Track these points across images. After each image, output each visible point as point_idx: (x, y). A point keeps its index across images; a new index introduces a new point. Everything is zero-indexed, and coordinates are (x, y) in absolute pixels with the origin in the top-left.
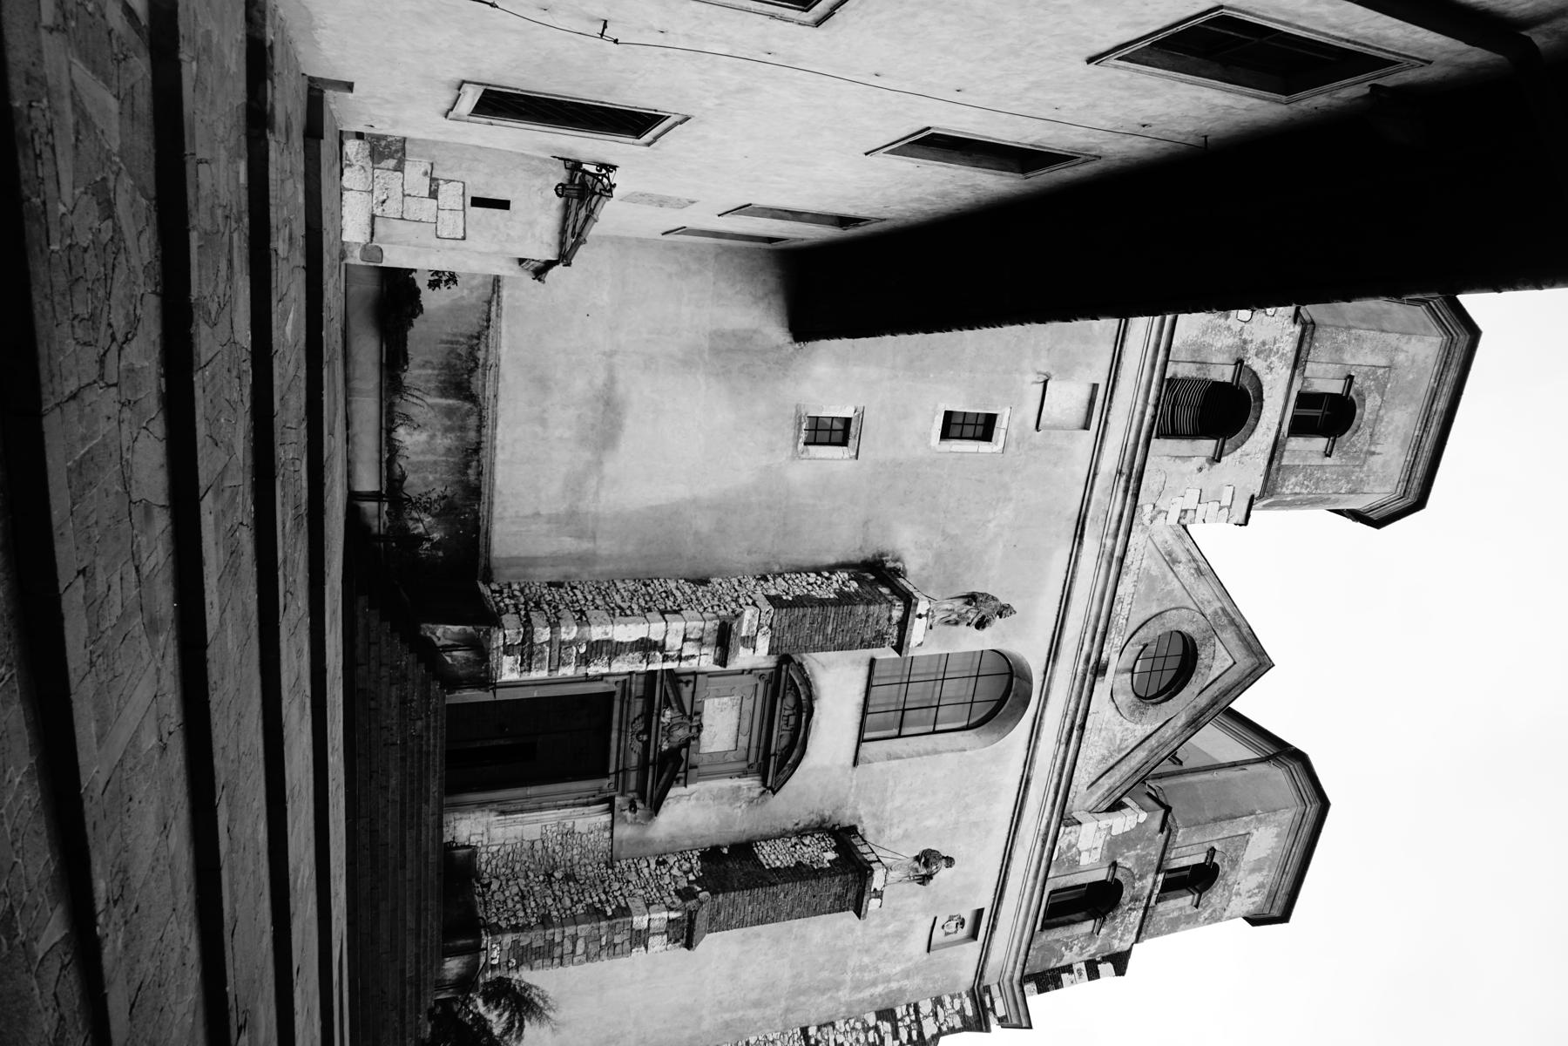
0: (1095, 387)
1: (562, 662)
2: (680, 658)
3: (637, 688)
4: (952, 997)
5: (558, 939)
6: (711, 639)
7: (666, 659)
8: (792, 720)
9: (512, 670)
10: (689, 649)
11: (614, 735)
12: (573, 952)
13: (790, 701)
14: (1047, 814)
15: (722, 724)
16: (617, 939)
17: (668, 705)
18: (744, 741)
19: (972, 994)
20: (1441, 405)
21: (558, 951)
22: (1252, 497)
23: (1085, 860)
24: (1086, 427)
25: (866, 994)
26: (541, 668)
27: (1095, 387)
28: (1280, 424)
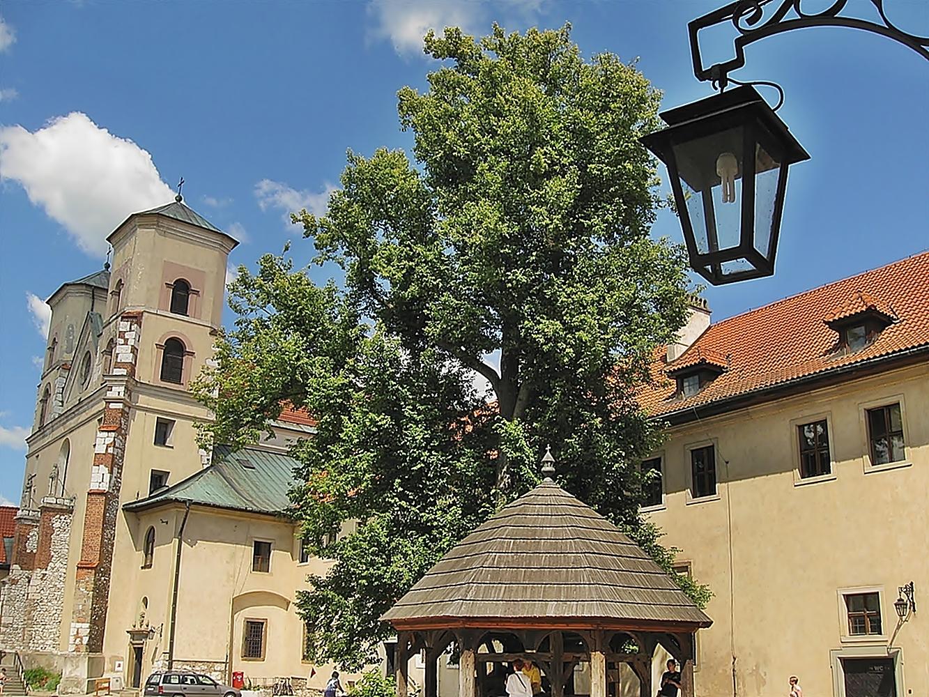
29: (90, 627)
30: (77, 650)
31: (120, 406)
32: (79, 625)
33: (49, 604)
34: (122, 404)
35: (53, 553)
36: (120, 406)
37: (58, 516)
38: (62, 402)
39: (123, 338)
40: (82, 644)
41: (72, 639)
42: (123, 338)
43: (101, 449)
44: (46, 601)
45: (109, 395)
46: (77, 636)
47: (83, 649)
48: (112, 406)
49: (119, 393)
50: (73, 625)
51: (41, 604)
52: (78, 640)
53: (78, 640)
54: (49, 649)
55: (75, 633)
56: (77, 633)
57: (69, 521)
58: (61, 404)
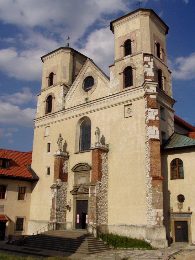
0: (46, 127)
1: (54, 212)
2: (55, 194)
3: (75, 196)
4: (145, 103)
5: (91, 211)
6: (53, 189)
7: (55, 196)
8: (82, 166)
9: (54, 220)
10: (54, 193)
11: (82, 199)
12: (93, 208)
13: (79, 167)
14: (105, 100)
15: (83, 181)
16: (93, 200)
17: (77, 191)
18: (85, 175)
19: (145, 98)
20: (50, 56)
21: (93, 211)
22: (60, 86)
23: (118, 83)
24: (49, 126)
25: (140, 129)
26: (55, 215)
27: (46, 127)
28: (51, 88)
29: (164, 211)
30: (158, 224)
31: (155, 97)
32: (158, 210)
33: (103, 199)
34: (156, 96)
35: (102, 173)
36: (155, 97)
37: (103, 154)
38: (65, 101)
39: (147, 64)
40: (160, 220)
41: (154, 218)
42: (147, 64)
43: (153, 118)
44: (102, 198)
45: (148, 91)
46: (157, 216)
47: (161, 223)
48: (151, 96)
49: (153, 90)
50: (154, 210)
51: (100, 199)
52: (158, 219)
53: (158, 219)
54: (104, 223)
55: (156, 215)
56: (157, 214)
57: (107, 156)
58: (64, 102)
